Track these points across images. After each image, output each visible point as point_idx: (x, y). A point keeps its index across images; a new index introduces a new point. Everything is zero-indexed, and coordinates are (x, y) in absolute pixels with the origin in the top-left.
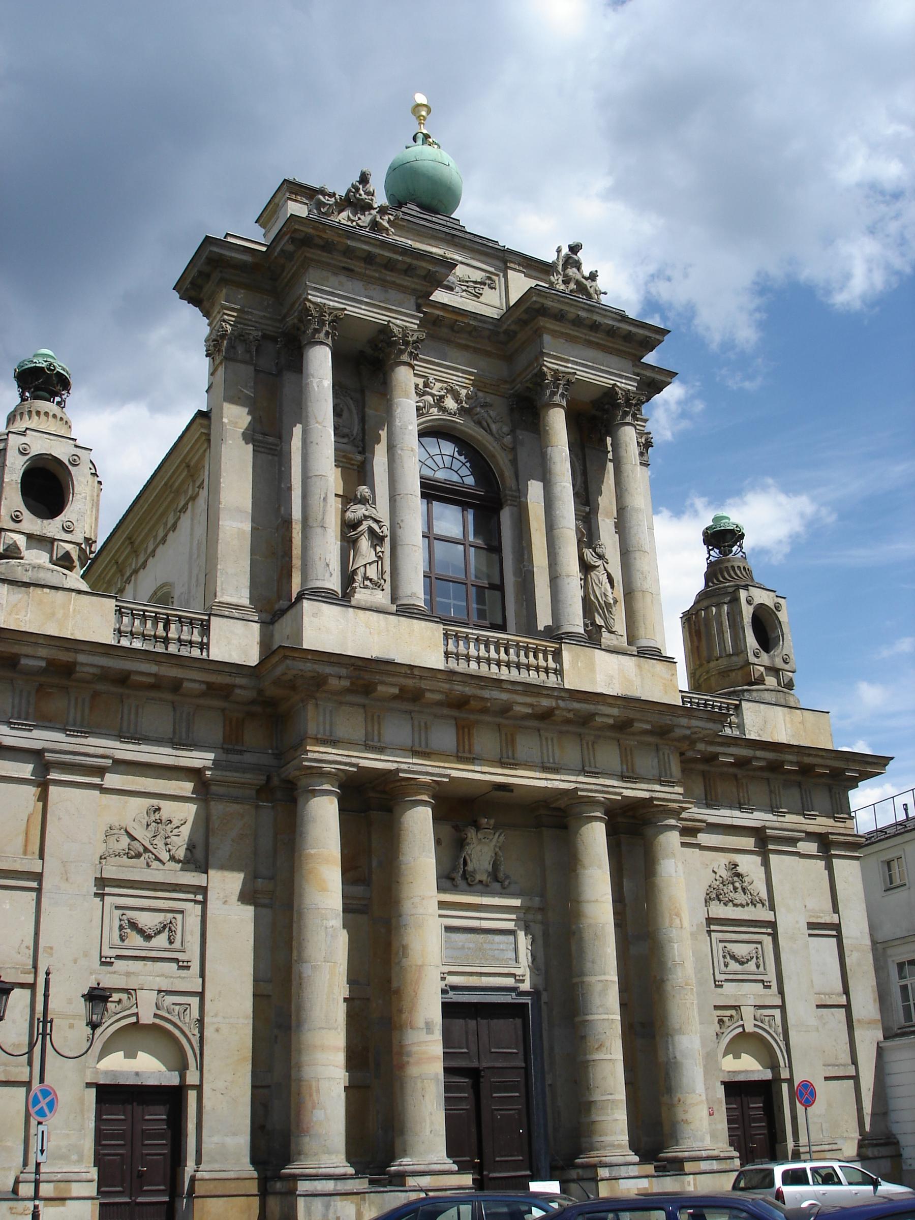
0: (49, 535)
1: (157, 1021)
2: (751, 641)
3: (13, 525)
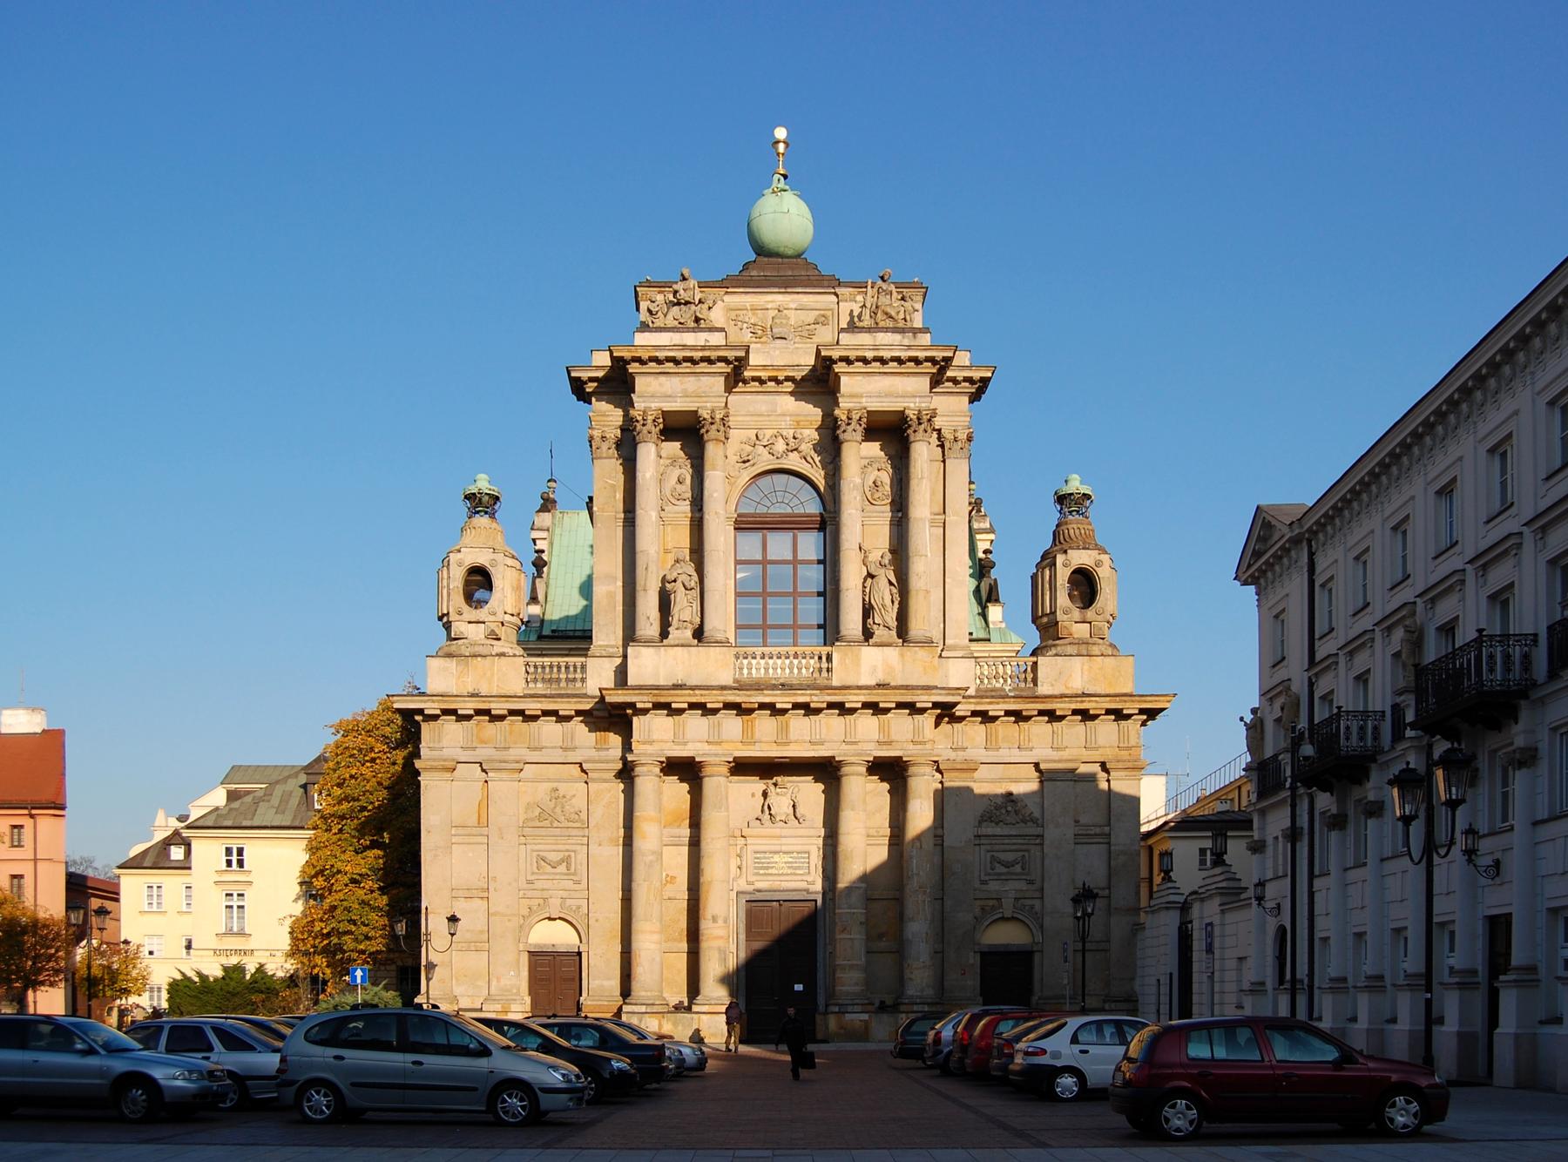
0: (481, 620)
1: (562, 916)
2: (1063, 599)
3: (458, 617)
